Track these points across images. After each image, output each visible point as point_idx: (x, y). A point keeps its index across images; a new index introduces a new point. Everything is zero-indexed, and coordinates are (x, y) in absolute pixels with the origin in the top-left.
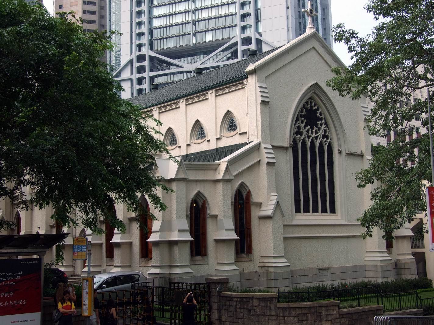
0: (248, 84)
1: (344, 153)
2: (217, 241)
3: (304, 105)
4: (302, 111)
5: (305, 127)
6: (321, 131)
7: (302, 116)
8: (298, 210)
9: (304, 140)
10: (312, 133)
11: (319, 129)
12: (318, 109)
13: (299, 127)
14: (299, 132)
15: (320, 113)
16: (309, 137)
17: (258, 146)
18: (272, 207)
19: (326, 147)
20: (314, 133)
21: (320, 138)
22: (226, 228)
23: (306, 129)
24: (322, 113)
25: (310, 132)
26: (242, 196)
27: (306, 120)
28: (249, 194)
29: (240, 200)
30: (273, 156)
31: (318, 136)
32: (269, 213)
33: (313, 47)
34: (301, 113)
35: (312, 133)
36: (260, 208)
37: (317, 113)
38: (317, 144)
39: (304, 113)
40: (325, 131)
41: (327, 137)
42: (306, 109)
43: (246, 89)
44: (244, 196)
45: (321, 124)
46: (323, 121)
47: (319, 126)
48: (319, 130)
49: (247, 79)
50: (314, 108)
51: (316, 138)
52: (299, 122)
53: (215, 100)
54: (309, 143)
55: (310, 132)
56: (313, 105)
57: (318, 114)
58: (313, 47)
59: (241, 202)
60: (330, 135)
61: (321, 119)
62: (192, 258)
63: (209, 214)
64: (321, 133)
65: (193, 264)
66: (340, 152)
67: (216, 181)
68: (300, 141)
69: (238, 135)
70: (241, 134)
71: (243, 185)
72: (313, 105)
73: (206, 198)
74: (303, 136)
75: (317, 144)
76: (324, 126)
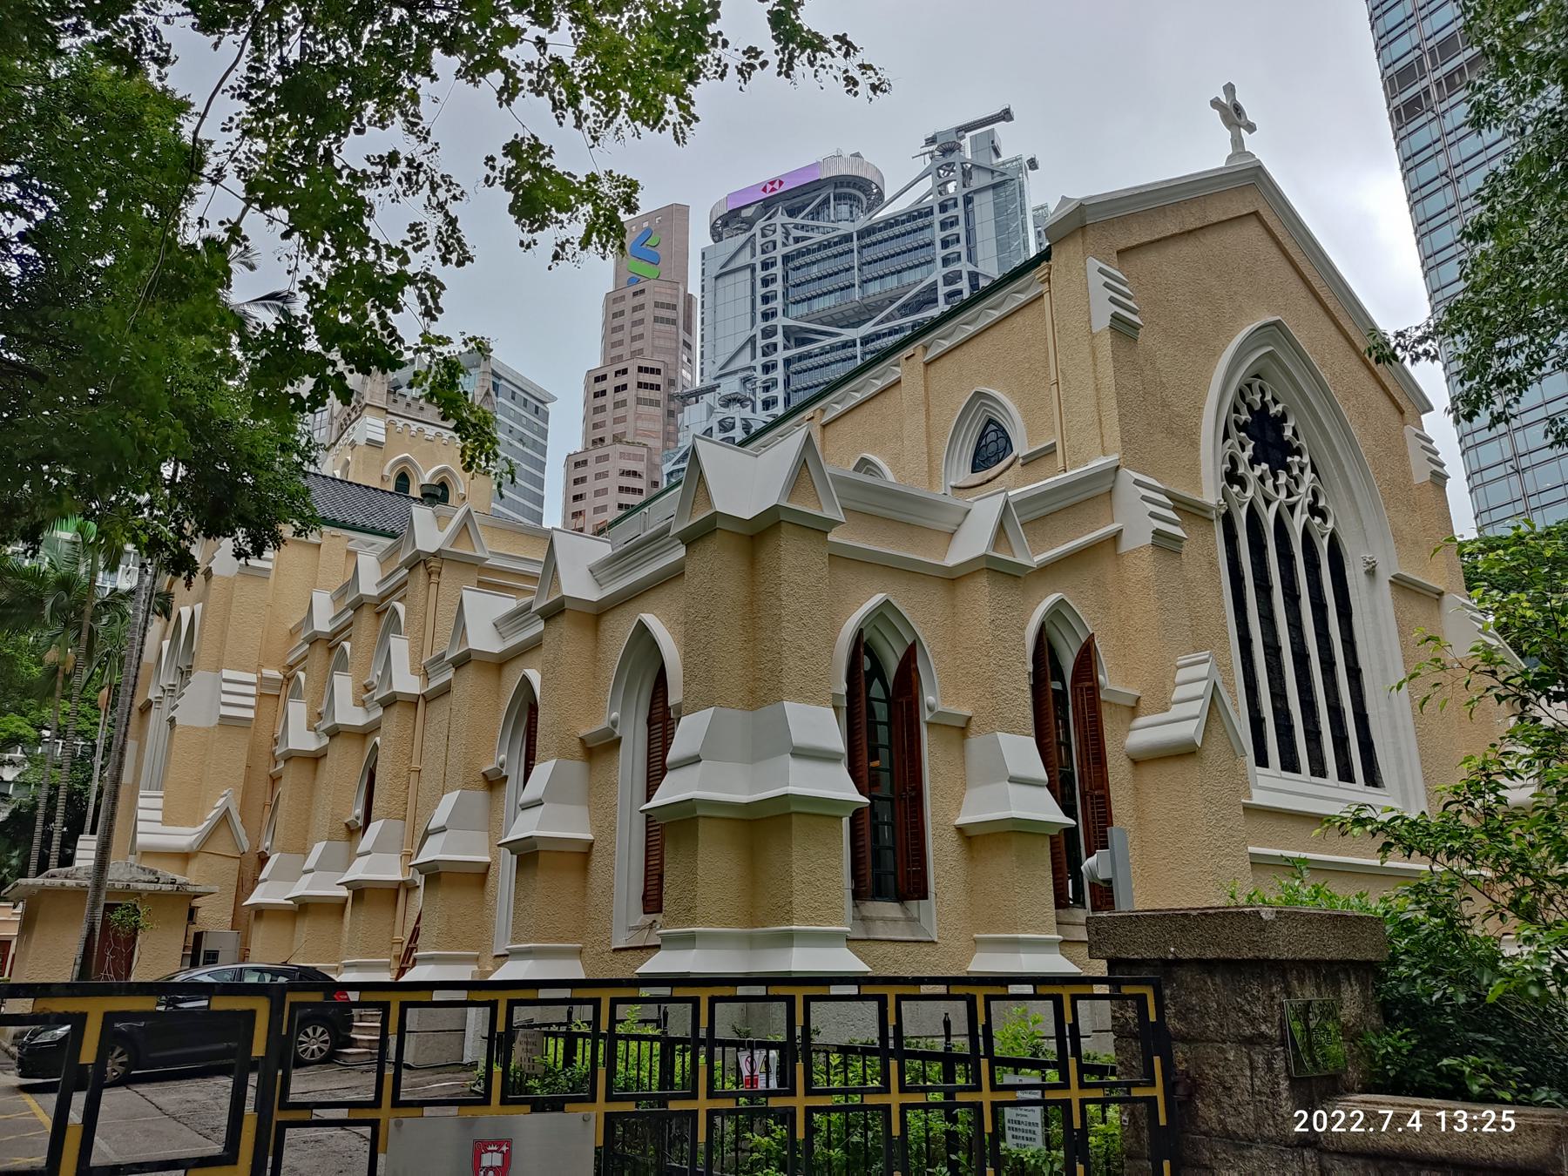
1: (1385, 576)
2: (970, 837)
3: (1242, 394)
4: (1236, 410)
5: (1254, 461)
6: (1302, 490)
7: (1240, 428)
8: (1262, 760)
12: (1283, 418)
13: (1233, 461)
14: (1233, 477)
15: (1294, 429)
16: (1268, 503)
18: (1197, 707)
19: (1323, 546)
20: (1283, 494)
22: (1013, 770)
23: (1258, 471)
24: (1300, 432)
25: (1269, 482)
29: (1053, 679)
32: (1190, 731)
33: (1256, 214)
38: (1297, 524)
39: (1245, 416)
40: (1315, 494)
41: (1323, 514)
43: (1047, 296)
45: (1302, 470)
46: (1306, 459)
47: (1296, 472)
51: (1292, 508)
52: (1229, 442)
54: (1269, 517)
55: (1269, 482)
56: (1268, 398)
57: (1288, 433)
58: (1256, 214)
59: (1057, 685)
61: (1299, 452)
62: (856, 906)
63: (931, 709)
64: (1303, 497)
65: (865, 937)
66: (1371, 573)
67: (953, 579)
69: (1017, 466)
70: (1030, 460)
72: (1268, 398)
74: (1250, 493)
76: (1308, 476)
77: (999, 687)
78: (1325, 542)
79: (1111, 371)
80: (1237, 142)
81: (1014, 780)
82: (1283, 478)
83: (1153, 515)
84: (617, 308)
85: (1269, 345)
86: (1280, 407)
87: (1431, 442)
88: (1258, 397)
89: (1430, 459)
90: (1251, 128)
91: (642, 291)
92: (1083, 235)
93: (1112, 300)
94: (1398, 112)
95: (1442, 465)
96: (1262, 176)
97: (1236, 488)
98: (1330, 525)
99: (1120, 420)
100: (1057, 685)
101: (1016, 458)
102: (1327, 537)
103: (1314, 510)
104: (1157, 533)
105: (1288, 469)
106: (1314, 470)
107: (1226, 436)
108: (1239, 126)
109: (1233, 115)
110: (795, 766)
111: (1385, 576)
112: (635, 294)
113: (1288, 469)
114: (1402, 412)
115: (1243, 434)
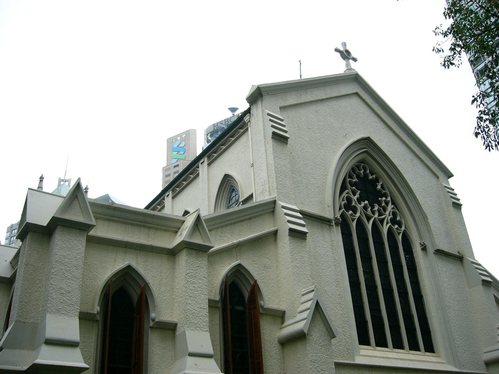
0: (253, 120)
3: (353, 169)
4: (350, 177)
5: (359, 200)
6: (387, 213)
7: (352, 184)
8: (364, 340)
9: (359, 221)
10: (373, 213)
11: (385, 210)
12: (377, 180)
13: (349, 199)
16: (369, 218)
17: (273, 206)
20: (376, 215)
21: (387, 223)
22: (191, 349)
23: (363, 205)
24: (385, 187)
25: (369, 209)
26: (242, 296)
27: (359, 191)
28: (255, 290)
30: (302, 222)
31: (384, 219)
32: (300, 326)
34: (348, 180)
35: (373, 213)
36: (283, 323)
37: (377, 186)
38: (385, 230)
39: (355, 180)
40: (394, 214)
41: (400, 224)
42: (358, 176)
44: (246, 295)
45: (387, 203)
46: (389, 199)
47: (383, 204)
48: (385, 211)
49: (250, 113)
50: (370, 177)
51: (382, 221)
52: (347, 191)
53: (208, 169)
54: (369, 226)
55: (369, 209)
57: (379, 187)
58: (357, 94)
60: (403, 221)
61: (385, 195)
66: (424, 249)
67: (172, 253)
68: (353, 220)
71: (239, 271)
72: (368, 171)
73: (147, 285)
74: (358, 215)
75: (385, 230)
77: (188, 307)
78: (400, 237)
79: (272, 158)
80: (348, 65)
81: (191, 355)
82: (376, 208)
83: (289, 222)
84: (167, 173)
85: (365, 148)
86: (374, 176)
87: (453, 190)
88: (362, 172)
89: (451, 197)
90: (355, 60)
91: (178, 165)
92: (262, 101)
93: (272, 126)
94: (477, 74)
95: (459, 200)
96: (358, 78)
97: (351, 212)
98: (403, 228)
99: (276, 179)
100: (240, 308)
101: (240, 202)
102: (401, 234)
103: (394, 221)
104: (291, 230)
105: (379, 204)
106: (393, 203)
107: (343, 188)
108: (349, 59)
109: (346, 55)
110: (45, 350)
111: (431, 250)
112: (175, 167)
113: (379, 204)
114: (438, 177)
115: (354, 188)
